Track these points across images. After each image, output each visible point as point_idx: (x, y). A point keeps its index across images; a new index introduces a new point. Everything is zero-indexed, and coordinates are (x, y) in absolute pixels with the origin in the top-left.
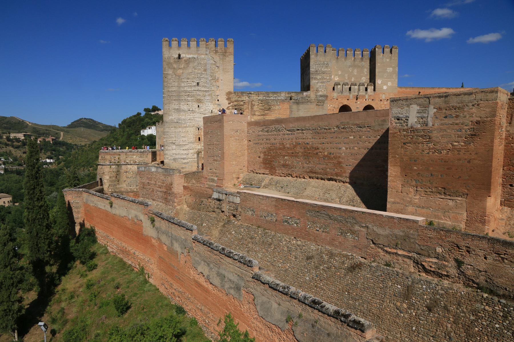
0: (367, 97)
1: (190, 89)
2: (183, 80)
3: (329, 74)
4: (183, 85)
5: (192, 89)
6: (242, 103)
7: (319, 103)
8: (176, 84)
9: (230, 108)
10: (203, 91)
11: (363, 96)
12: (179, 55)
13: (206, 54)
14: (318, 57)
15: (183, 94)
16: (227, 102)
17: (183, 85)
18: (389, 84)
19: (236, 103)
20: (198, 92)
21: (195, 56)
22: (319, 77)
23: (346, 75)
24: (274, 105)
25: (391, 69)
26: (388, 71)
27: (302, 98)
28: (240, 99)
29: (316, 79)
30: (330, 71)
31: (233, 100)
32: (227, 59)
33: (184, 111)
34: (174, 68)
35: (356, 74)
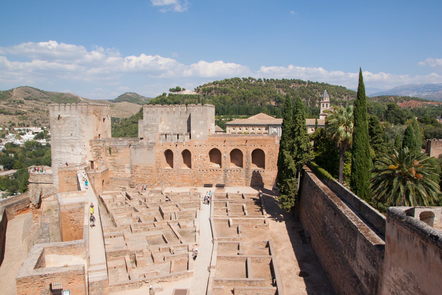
0: (184, 144)
1: (67, 138)
2: (62, 132)
3: (157, 126)
4: (62, 135)
5: (68, 138)
6: (99, 148)
7: (150, 149)
8: (58, 135)
9: (92, 151)
10: (75, 139)
11: (182, 143)
12: (59, 116)
13: (76, 114)
14: (149, 115)
15: (63, 141)
16: (90, 147)
17: (62, 135)
18: (202, 133)
19: (95, 148)
20: (71, 140)
21: (69, 116)
22: (149, 129)
23: (175, 125)
24: (120, 149)
25: (203, 122)
26: (201, 123)
27: (138, 144)
28: (98, 145)
29: (147, 130)
30: (157, 124)
31: (94, 145)
32: (89, 117)
33: (64, 153)
34: (57, 124)
35: (182, 124)
